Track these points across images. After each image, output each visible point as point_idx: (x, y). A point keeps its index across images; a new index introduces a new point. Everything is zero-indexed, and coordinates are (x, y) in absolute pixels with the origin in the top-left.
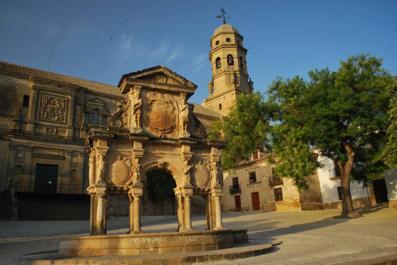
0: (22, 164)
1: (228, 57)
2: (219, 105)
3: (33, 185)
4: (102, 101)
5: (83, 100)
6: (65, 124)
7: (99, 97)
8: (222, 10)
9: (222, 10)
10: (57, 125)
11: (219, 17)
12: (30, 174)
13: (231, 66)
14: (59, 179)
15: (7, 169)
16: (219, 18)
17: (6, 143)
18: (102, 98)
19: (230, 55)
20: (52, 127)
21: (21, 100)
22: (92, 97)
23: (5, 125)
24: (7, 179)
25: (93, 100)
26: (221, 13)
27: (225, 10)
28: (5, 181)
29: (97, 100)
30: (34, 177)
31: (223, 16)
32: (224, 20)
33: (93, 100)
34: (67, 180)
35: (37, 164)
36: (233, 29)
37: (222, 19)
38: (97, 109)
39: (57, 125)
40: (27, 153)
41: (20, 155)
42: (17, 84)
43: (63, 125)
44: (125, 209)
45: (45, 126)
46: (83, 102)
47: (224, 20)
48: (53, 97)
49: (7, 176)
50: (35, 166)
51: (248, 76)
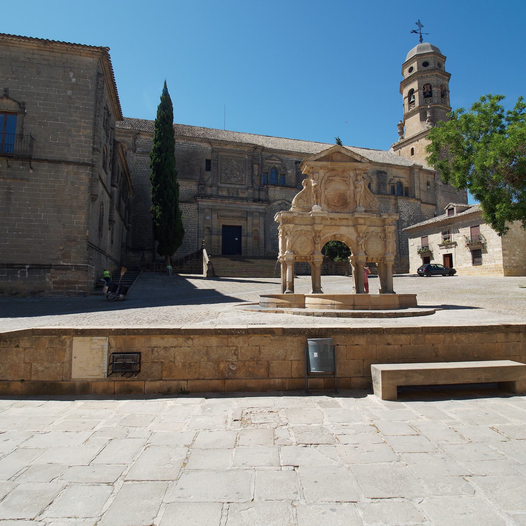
0: (210, 226)
1: (424, 87)
2: (410, 150)
3: (221, 244)
4: (278, 158)
5: (260, 159)
6: (245, 185)
7: (276, 154)
8: (418, 23)
9: (418, 23)
10: (238, 186)
11: (415, 32)
12: (217, 235)
13: (428, 99)
14: (243, 239)
15: (198, 230)
16: (414, 33)
17: (194, 206)
18: (279, 155)
19: (428, 84)
20: (233, 188)
21: (204, 165)
22: (268, 154)
23: (192, 189)
24: (198, 239)
25: (268, 158)
26: (416, 28)
27: (422, 23)
28: (197, 242)
29: (274, 158)
30: (221, 237)
31: (419, 32)
32: (421, 37)
33: (268, 158)
34: (250, 239)
35: (223, 226)
36: (433, 47)
37: (419, 35)
38: (275, 168)
39: (238, 186)
40: (213, 215)
41: (208, 218)
42: (198, 149)
43: (244, 187)
44: (305, 268)
45: (225, 187)
46: (260, 161)
47: (421, 37)
48: (232, 158)
49: (198, 237)
50: (221, 228)
51: (451, 108)
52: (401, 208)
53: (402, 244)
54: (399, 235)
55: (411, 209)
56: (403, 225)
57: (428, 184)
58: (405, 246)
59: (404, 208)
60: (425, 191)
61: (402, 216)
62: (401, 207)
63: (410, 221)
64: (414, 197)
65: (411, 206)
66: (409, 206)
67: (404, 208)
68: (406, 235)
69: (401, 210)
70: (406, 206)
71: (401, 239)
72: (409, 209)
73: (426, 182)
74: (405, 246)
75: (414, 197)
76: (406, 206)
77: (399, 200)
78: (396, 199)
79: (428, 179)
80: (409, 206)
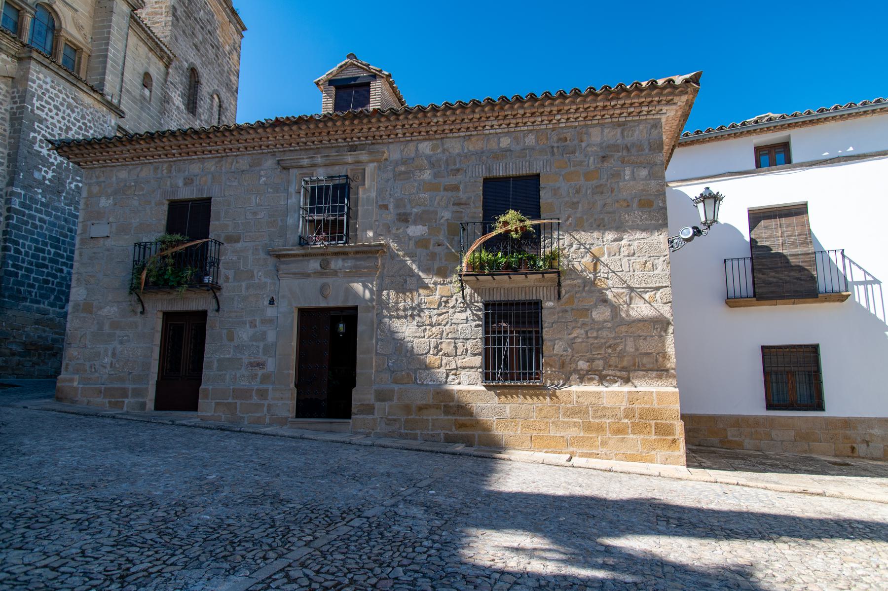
52: (37, 104)
53: (17, 251)
54: (9, 210)
55: (80, 128)
56: (37, 175)
57: (147, 80)
58: (31, 263)
59: (50, 111)
60: (134, 97)
61: (39, 137)
62: (40, 98)
63: (67, 169)
64: (97, 90)
65: (83, 117)
66: (73, 112)
67: (50, 111)
68: (41, 220)
69: (37, 112)
70: (62, 104)
71: (15, 227)
72: (74, 125)
73: (142, 72)
74: (31, 263)
75: (97, 90)
76: (62, 104)
77: (34, 66)
78: (20, 59)
79: (149, 64)
80: (73, 112)
